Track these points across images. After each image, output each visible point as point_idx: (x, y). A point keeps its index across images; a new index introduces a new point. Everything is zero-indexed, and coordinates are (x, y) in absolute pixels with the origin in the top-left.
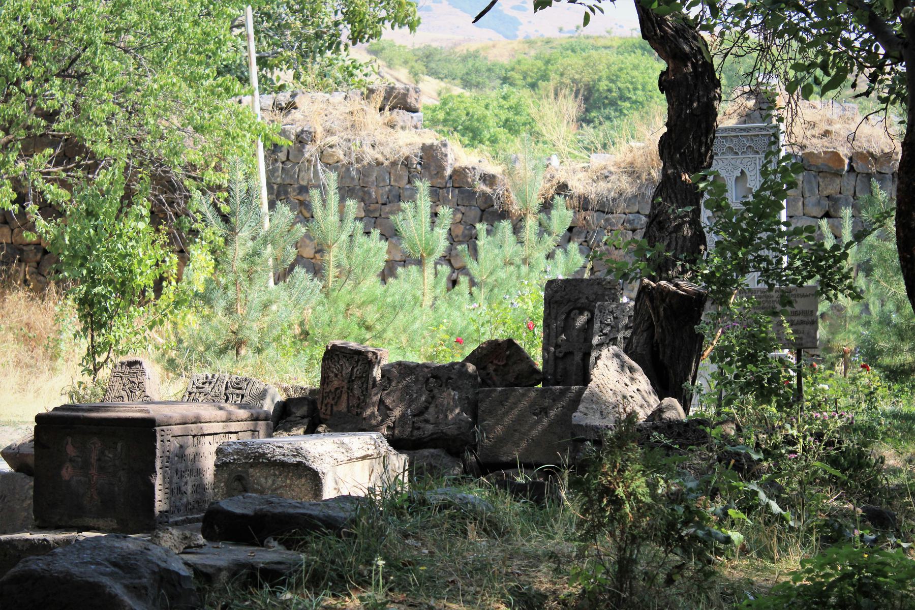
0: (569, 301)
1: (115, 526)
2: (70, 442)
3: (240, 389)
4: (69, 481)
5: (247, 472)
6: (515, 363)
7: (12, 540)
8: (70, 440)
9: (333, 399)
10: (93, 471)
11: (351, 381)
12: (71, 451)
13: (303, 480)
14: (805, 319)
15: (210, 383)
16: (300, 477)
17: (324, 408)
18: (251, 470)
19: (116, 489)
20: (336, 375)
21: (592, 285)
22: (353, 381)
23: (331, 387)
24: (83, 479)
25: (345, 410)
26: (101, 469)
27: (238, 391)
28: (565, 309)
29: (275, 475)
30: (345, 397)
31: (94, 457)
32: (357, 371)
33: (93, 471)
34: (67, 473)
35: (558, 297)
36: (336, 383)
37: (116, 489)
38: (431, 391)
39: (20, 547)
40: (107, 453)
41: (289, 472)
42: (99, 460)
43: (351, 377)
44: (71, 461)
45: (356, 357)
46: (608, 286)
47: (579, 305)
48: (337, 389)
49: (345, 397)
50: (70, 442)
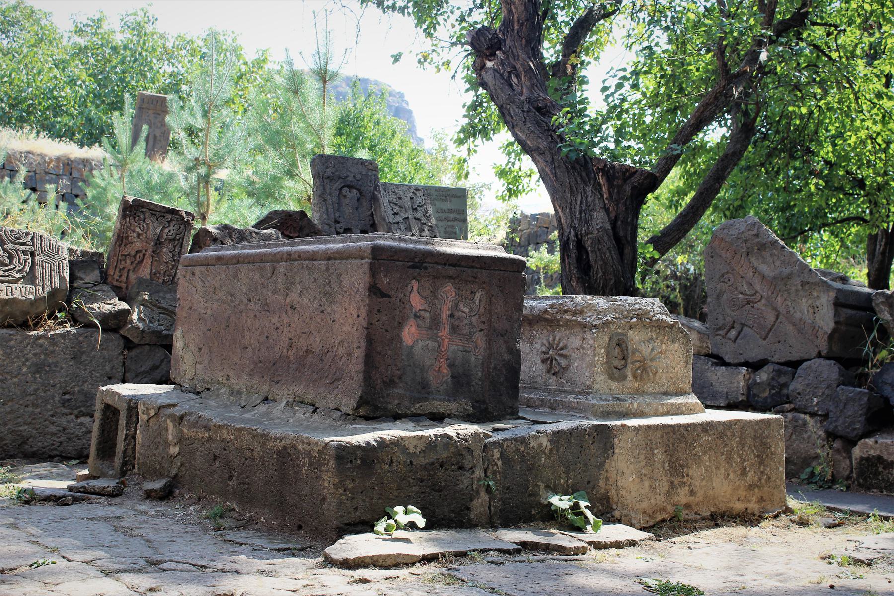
0: (340, 178)
1: (471, 411)
2: (415, 289)
3: (24, 244)
4: (412, 347)
5: (626, 335)
7: (397, 442)
8: (415, 284)
9: (132, 263)
10: (444, 333)
11: (159, 243)
12: (416, 302)
13: (676, 345)
14: (458, 216)
16: (674, 341)
17: (117, 273)
18: (631, 332)
19: (473, 358)
20: (139, 236)
21: (357, 164)
22: (161, 243)
24: (432, 344)
25: (149, 277)
26: (455, 329)
27: (23, 248)
28: (338, 185)
29: (652, 339)
30: (148, 261)
31: (445, 313)
32: (171, 231)
33: (444, 333)
34: (410, 333)
35: (329, 172)
36: (138, 245)
37: (473, 358)
39: (412, 450)
40: (461, 306)
41: (664, 335)
42: (452, 316)
43: (158, 240)
44: (416, 316)
45: (169, 216)
46: (370, 167)
47: (349, 183)
48: (137, 252)
49: (148, 261)
50: (415, 289)
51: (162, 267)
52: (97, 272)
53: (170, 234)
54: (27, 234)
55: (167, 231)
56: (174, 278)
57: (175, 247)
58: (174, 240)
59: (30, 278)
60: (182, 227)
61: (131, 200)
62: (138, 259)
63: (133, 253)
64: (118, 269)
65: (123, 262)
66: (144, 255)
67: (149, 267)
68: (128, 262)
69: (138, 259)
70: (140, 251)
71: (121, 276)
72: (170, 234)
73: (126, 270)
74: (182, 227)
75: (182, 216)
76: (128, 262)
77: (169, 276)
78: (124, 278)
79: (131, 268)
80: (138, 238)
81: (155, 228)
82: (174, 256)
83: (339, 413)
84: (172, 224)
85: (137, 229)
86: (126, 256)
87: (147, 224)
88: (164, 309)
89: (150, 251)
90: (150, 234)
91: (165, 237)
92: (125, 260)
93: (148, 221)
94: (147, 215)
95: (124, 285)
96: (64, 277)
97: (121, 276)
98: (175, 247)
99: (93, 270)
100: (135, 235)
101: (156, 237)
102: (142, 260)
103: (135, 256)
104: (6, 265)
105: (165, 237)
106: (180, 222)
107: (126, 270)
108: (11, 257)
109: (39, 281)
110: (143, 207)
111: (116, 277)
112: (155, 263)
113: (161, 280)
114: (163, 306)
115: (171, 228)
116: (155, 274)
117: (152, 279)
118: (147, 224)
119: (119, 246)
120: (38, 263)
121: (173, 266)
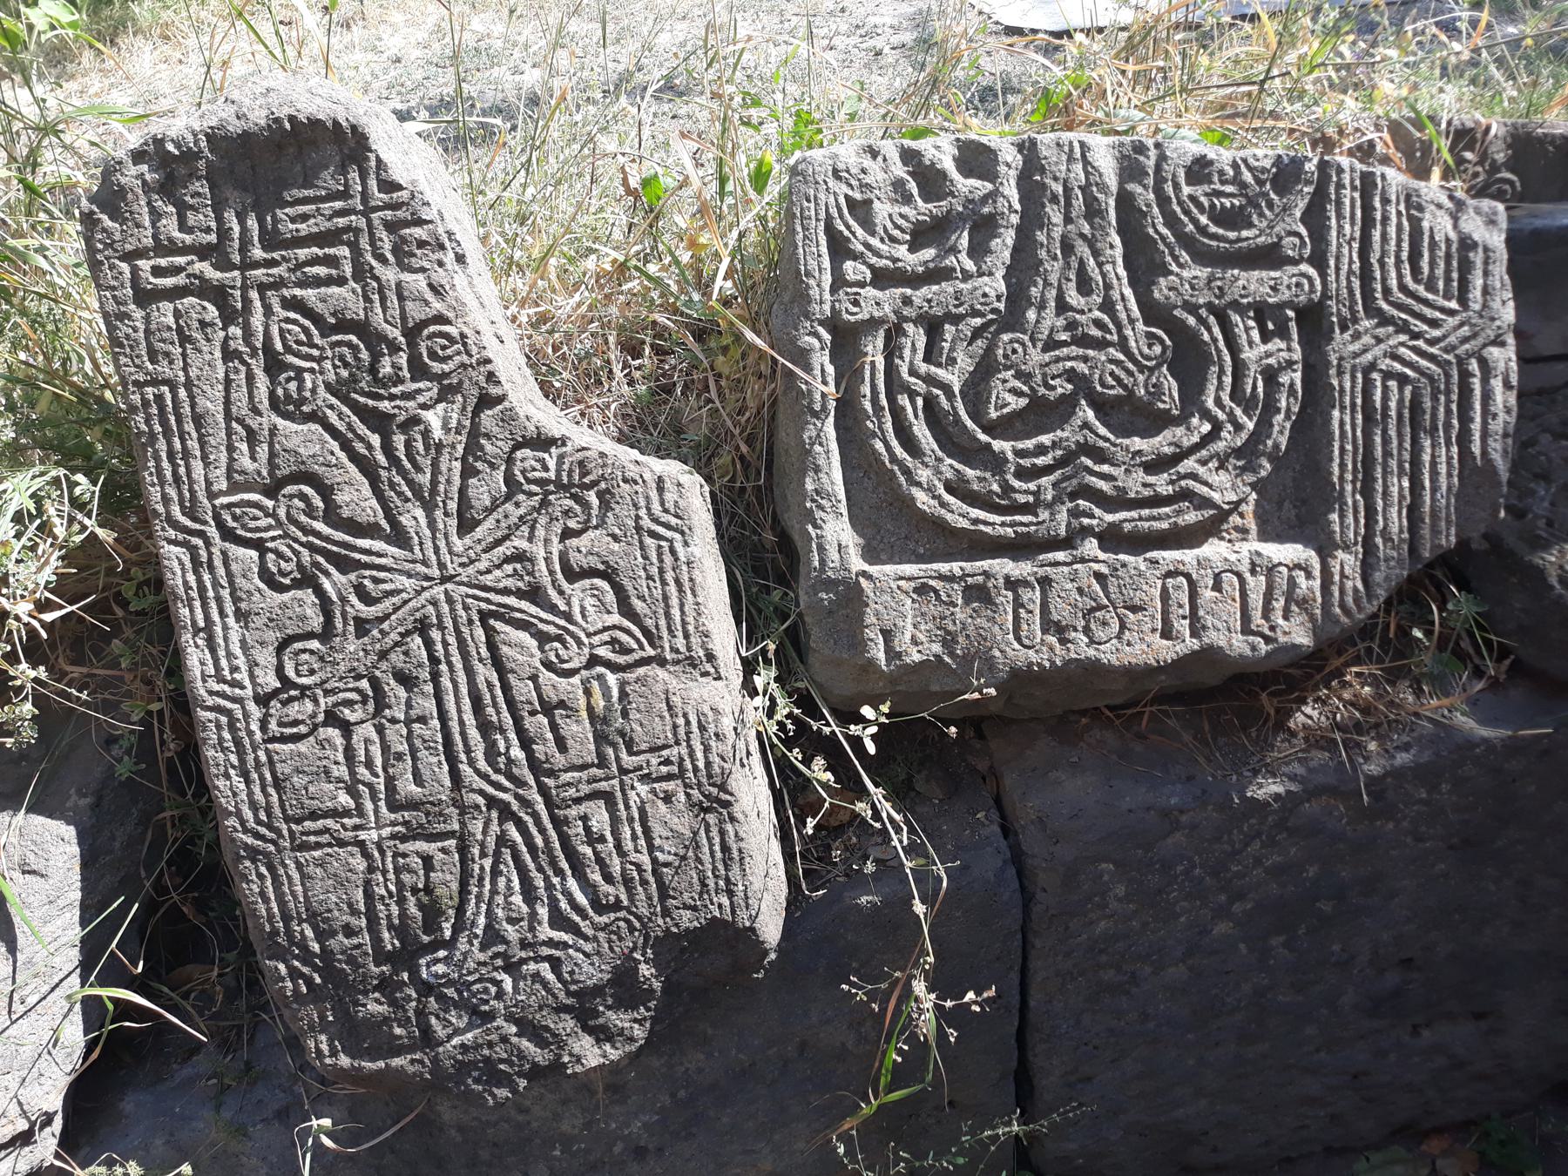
3: (1269, 257)
15: (984, 227)
27: (1254, 283)
54: (1286, 175)
59: (1295, 504)
104: (1155, 422)
108: (1189, 361)
109: (1345, 523)
120: (1345, 385)
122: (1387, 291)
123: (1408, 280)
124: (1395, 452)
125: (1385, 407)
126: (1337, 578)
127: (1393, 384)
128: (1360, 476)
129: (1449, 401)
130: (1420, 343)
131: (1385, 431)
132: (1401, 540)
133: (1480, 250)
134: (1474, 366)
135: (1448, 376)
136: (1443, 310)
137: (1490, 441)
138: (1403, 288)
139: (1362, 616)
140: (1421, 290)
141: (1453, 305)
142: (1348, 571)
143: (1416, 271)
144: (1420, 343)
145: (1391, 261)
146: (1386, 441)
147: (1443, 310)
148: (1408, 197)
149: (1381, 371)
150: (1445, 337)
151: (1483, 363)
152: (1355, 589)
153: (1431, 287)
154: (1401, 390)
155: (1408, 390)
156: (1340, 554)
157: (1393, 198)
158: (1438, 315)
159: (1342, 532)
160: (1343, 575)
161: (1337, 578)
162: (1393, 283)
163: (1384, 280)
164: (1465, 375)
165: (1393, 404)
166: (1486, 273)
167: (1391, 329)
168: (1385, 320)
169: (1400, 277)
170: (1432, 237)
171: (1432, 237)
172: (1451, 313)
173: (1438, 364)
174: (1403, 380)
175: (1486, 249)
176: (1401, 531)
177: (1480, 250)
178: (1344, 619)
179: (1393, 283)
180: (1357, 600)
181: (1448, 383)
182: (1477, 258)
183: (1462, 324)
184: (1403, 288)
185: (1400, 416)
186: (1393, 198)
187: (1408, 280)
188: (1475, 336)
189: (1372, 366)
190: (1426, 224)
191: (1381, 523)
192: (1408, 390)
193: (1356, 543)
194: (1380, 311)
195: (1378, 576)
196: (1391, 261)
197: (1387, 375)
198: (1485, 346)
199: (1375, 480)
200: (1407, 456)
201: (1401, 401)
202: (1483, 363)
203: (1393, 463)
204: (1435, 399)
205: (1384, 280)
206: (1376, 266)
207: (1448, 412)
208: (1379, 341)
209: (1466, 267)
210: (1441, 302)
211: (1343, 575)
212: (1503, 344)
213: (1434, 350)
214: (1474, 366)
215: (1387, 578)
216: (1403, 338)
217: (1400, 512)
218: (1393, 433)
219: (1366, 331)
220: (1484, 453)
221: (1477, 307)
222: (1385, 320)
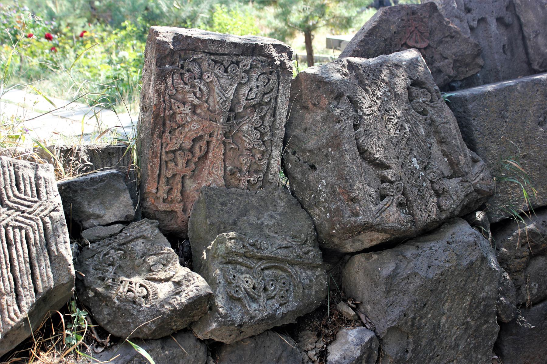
6: (441, 42)
9: (188, 162)
17: (164, 187)
20: (194, 107)
23: (182, 139)
36: (195, 127)
38: (423, 113)
43: (231, 110)
45: (247, 61)
49: (217, 153)
51: (243, 159)
52: (126, 198)
53: (252, 95)
55: (245, 90)
56: (266, 174)
57: (262, 118)
58: (260, 104)
60: (273, 77)
61: (169, 39)
62: (198, 154)
63: (187, 145)
64: (163, 180)
65: (171, 165)
66: (208, 143)
67: (220, 163)
68: (181, 162)
69: (198, 154)
70: (201, 137)
71: (169, 191)
72: (252, 95)
73: (178, 178)
74: (273, 77)
75: (269, 56)
76: (181, 162)
77: (257, 172)
78: (176, 194)
79: (188, 172)
80: (194, 112)
81: (222, 89)
82: (262, 134)
83: (412, 219)
84: (254, 76)
85: (190, 97)
86: (174, 152)
87: (207, 84)
88: (269, 258)
89: (219, 133)
90: (216, 101)
91: (243, 103)
92: (174, 160)
93: (209, 77)
94: (205, 66)
95: (178, 207)
96: (61, 257)
97: (169, 191)
98: (262, 118)
99: (117, 196)
100: (187, 109)
101: (228, 105)
102: (207, 152)
103: (191, 150)
105: (243, 103)
106: (268, 69)
107: (178, 178)
110: (195, 50)
111: (162, 194)
112: (230, 154)
113: (244, 184)
114: (268, 253)
115: (253, 84)
116: (233, 174)
117: (228, 186)
118: (207, 84)
119: (160, 137)
121: (263, 153)
122: (9, 198)
123: (17, 193)
124: (22, 255)
125: (15, 239)
126: (5, 307)
127: (17, 230)
128: (9, 266)
129: (40, 233)
130: (26, 214)
131: (16, 248)
132: (30, 287)
133: (43, 179)
134: (47, 219)
135: (37, 224)
136: (32, 202)
137: (59, 245)
138: (15, 196)
139: (19, 320)
140: (22, 196)
141: (36, 199)
142: (9, 303)
143: (19, 189)
144: (26, 214)
145: (9, 187)
146: (17, 252)
147: (32, 202)
148: (14, 165)
149: (11, 226)
150: (34, 211)
151: (51, 218)
152: (14, 310)
153: (25, 194)
154: (20, 231)
155: (23, 232)
156: (6, 297)
157: (6, 165)
158: (30, 203)
159: (5, 288)
160: (8, 305)
161: (5, 307)
162: (11, 194)
163: (7, 194)
164: (44, 224)
165: (18, 238)
166: (46, 187)
167: (13, 211)
168: (10, 208)
169: (13, 192)
170: (23, 177)
171: (23, 177)
172: (36, 202)
173: (34, 220)
174: (21, 228)
175: (45, 179)
176: (29, 284)
177: (43, 179)
178: (12, 323)
179: (11, 194)
180: (16, 314)
181: (38, 227)
182: (42, 182)
183: (40, 206)
184: (15, 196)
185: (22, 241)
186: (6, 165)
187: (17, 193)
188: (46, 209)
189: (7, 225)
190: (20, 173)
191: (21, 282)
192: (23, 232)
193: (11, 292)
194: (7, 205)
195: (23, 303)
196: (9, 187)
197: (14, 227)
198: (50, 212)
199: (15, 266)
200: (27, 255)
201: (21, 236)
202: (51, 218)
203: (22, 259)
204: (34, 233)
205: (7, 194)
206: (3, 190)
207: (40, 237)
208: (9, 216)
209: (38, 186)
210: (30, 198)
211: (8, 305)
212: (58, 211)
213: (31, 216)
214: (47, 219)
215: (27, 303)
216: (19, 213)
217: (27, 276)
218: (19, 247)
219: (3, 213)
220: (58, 250)
221: (45, 199)
222: (10, 208)
